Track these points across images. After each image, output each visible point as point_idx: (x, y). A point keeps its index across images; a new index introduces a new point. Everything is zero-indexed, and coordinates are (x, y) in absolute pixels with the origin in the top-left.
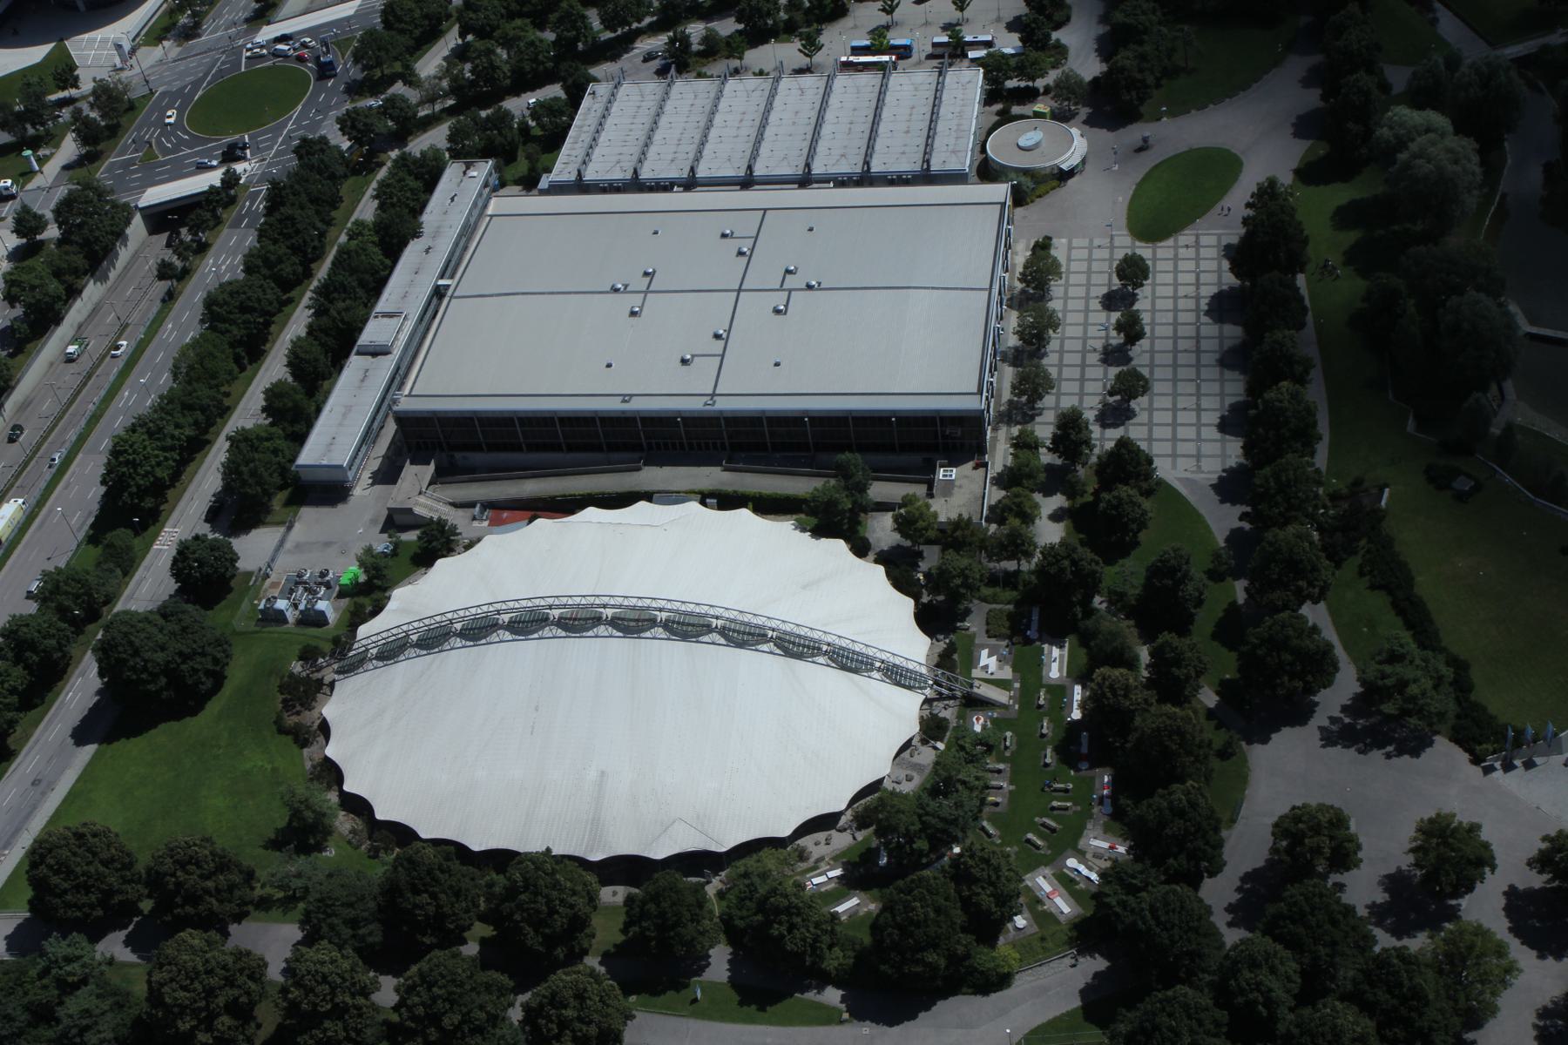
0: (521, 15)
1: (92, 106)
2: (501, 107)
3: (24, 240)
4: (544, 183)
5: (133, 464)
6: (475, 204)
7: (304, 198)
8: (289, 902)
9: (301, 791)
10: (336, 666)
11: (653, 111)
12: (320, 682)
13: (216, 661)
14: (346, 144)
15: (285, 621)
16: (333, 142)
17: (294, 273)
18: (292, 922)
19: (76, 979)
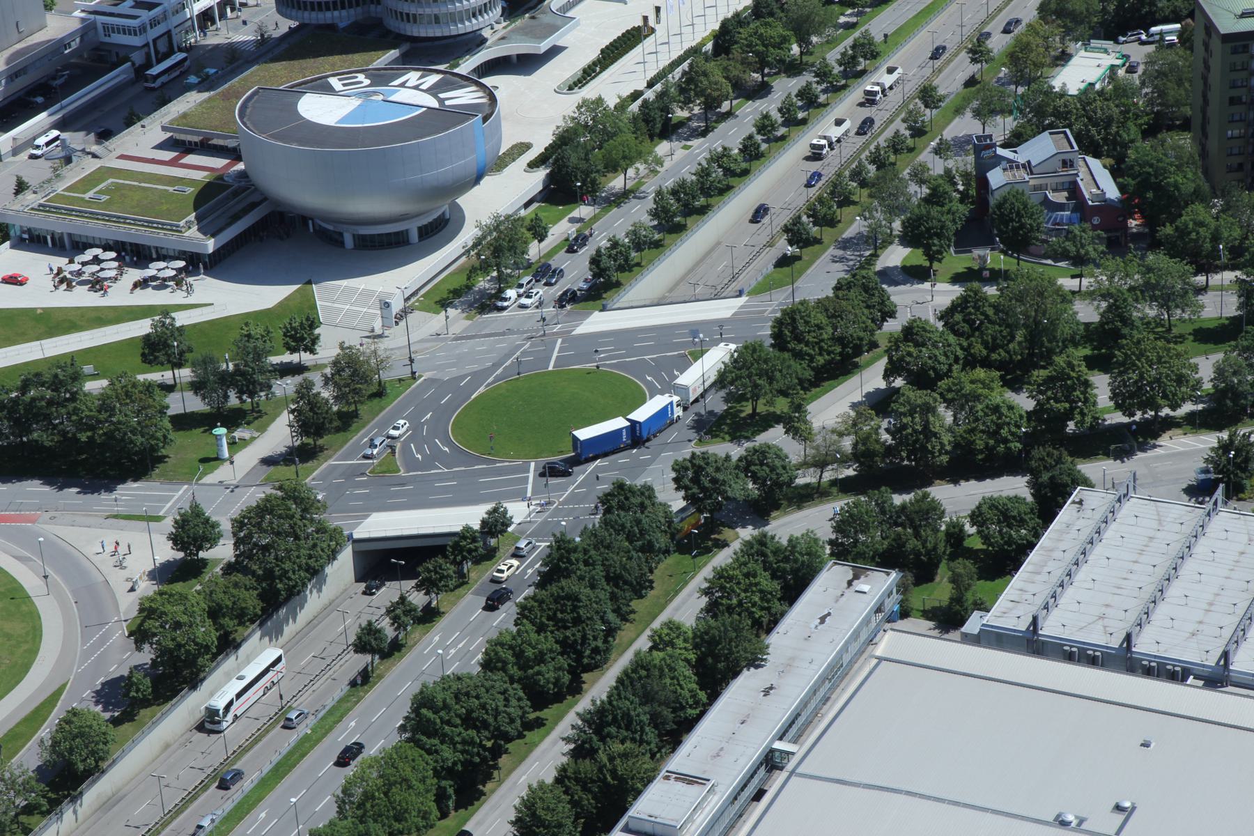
0: (986, 363)
1: (327, 381)
2: (926, 496)
3: (181, 555)
4: (974, 624)
6: (856, 635)
7: (599, 572)
11: (1175, 548)
14: (677, 502)
16: (661, 497)
17: (557, 682)
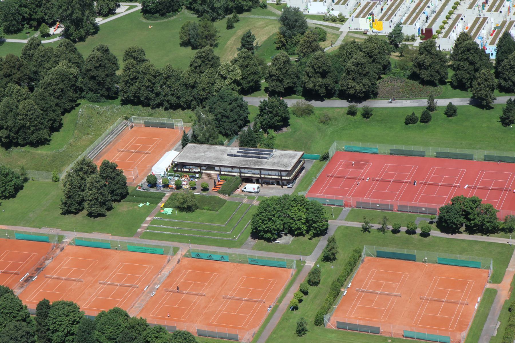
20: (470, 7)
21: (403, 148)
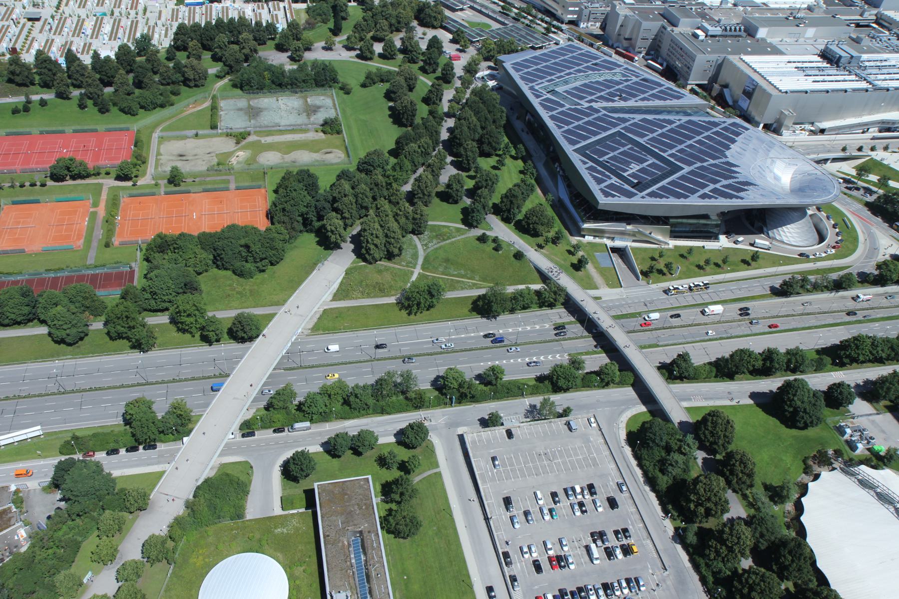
5: (857, 347)
8: (751, 505)
9: (791, 485)
10: (842, 466)
12: (831, 464)
13: (812, 422)
15: (843, 436)
18: (746, 510)
19: (684, 451)
20: (41, 32)
21: (15, 130)
